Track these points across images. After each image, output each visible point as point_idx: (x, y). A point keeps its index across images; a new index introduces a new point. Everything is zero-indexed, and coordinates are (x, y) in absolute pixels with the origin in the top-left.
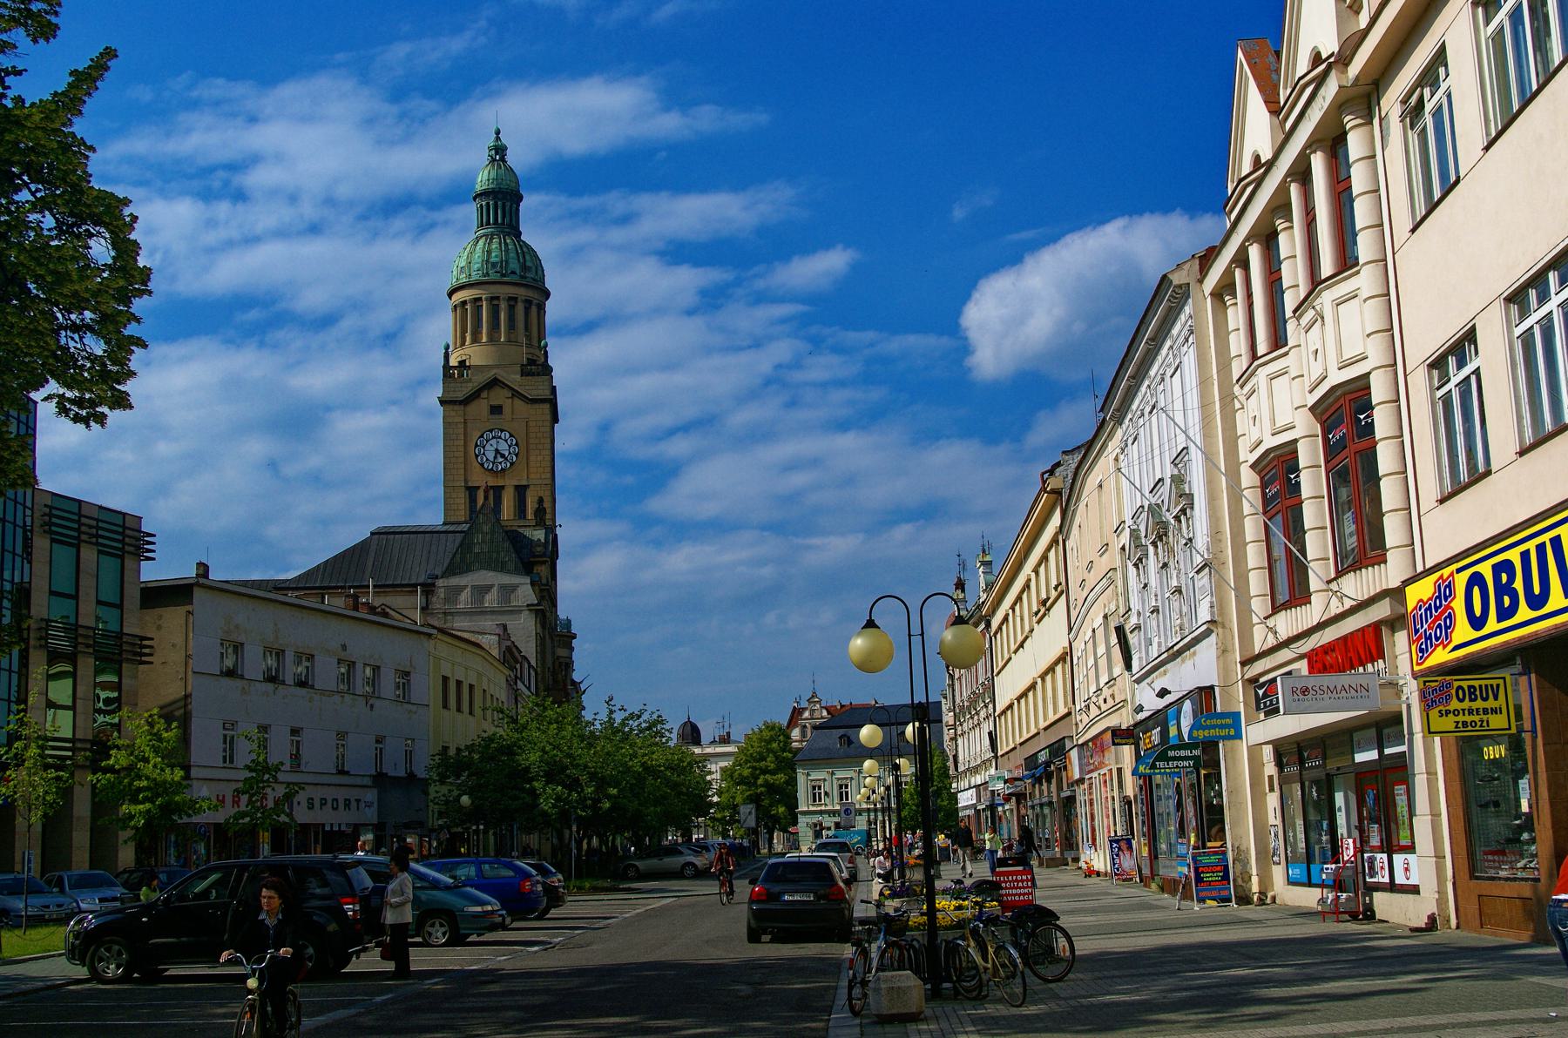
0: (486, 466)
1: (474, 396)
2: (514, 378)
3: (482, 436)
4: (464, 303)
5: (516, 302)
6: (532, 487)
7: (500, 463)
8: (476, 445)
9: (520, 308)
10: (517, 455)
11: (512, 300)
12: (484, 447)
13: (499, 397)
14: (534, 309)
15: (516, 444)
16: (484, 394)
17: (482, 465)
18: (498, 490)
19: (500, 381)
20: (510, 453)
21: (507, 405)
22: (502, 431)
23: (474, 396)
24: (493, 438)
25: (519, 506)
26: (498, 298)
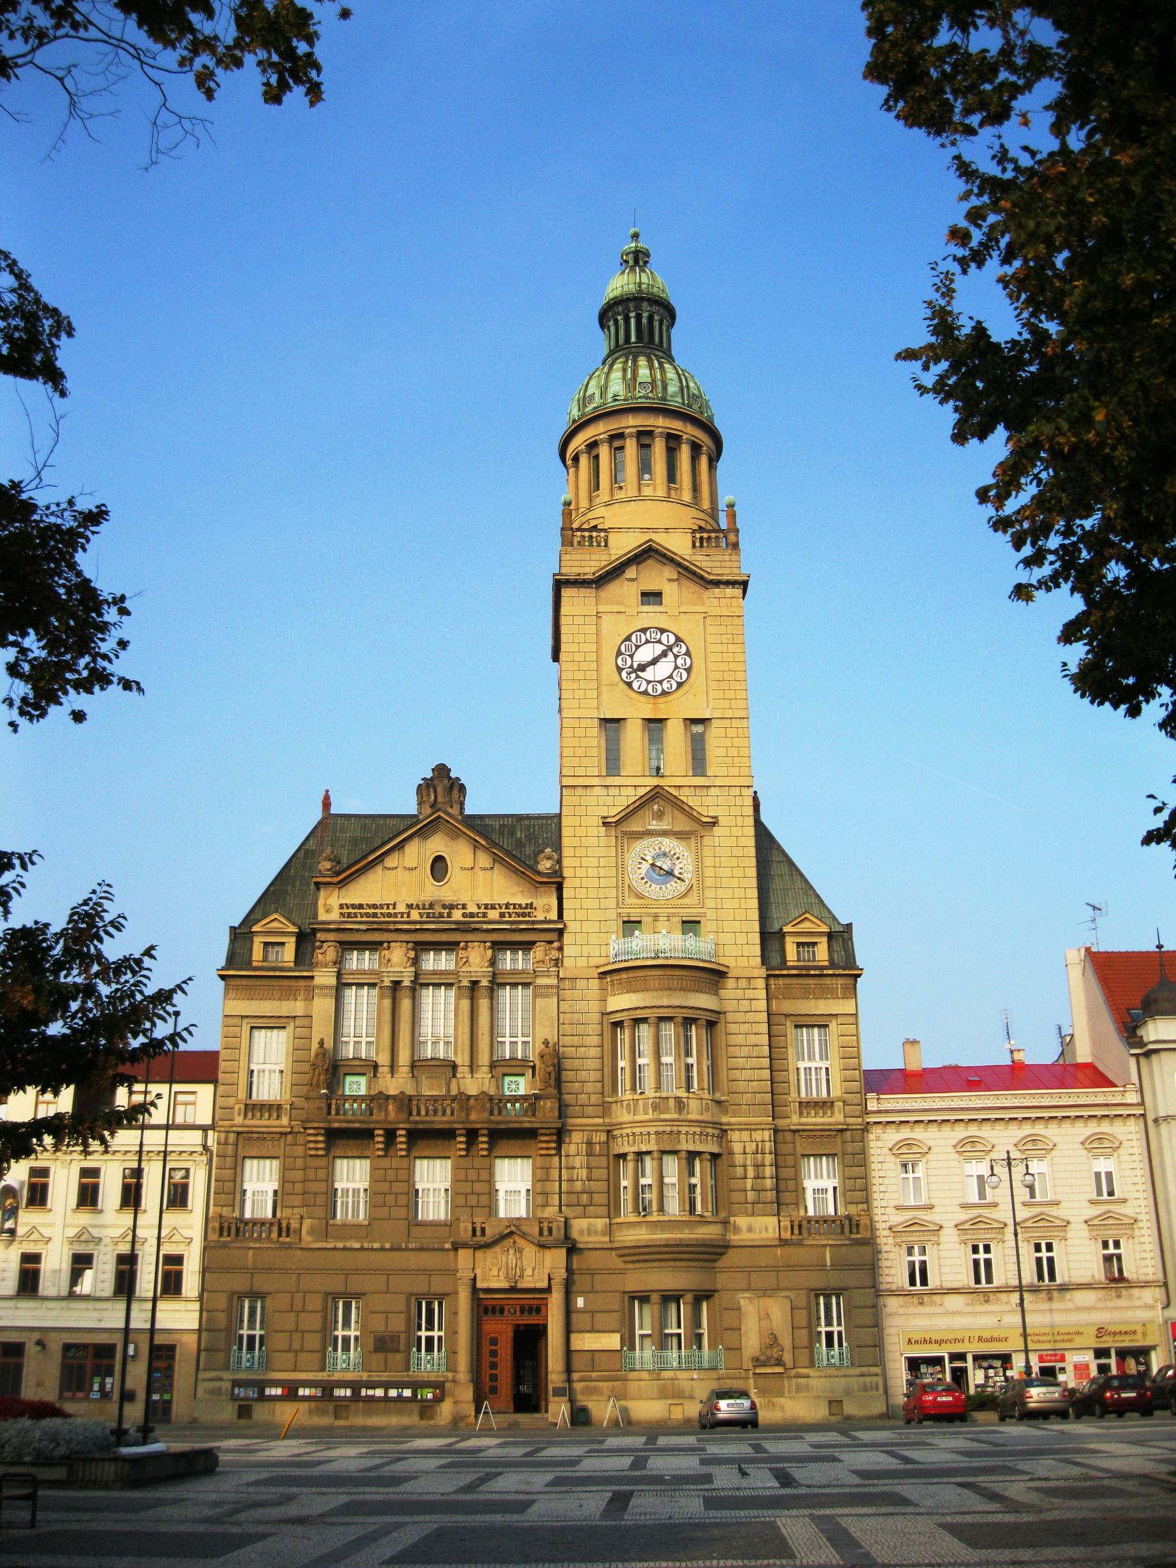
0: (635, 685)
1: (614, 573)
2: (679, 544)
3: (628, 638)
4: (593, 445)
5: (680, 444)
6: (715, 723)
7: (661, 682)
8: (619, 653)
9: (685, 453)
10: (689, 670)
11: (673, 441)
12: (631, 656)
13: (656, 577)
14: (704, 461)
15: (688, 653)
16: (631, 572)
17: (629, 684)
18: (655, 725)
19: (657, 551)
20: (676, 667)
21: (670, 592)
22: (663, 631)
23: (614, 573)
24: (647, 642)
25: (694, 751)
26: (650, 434)
